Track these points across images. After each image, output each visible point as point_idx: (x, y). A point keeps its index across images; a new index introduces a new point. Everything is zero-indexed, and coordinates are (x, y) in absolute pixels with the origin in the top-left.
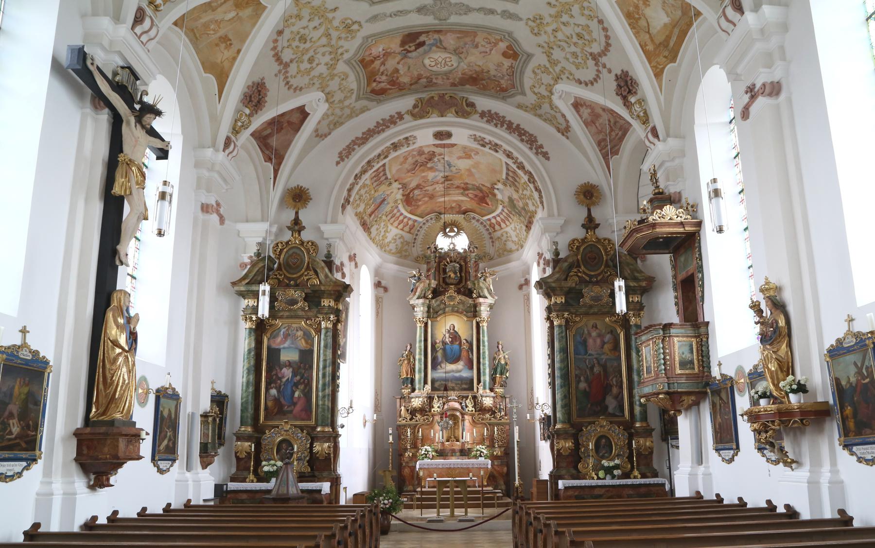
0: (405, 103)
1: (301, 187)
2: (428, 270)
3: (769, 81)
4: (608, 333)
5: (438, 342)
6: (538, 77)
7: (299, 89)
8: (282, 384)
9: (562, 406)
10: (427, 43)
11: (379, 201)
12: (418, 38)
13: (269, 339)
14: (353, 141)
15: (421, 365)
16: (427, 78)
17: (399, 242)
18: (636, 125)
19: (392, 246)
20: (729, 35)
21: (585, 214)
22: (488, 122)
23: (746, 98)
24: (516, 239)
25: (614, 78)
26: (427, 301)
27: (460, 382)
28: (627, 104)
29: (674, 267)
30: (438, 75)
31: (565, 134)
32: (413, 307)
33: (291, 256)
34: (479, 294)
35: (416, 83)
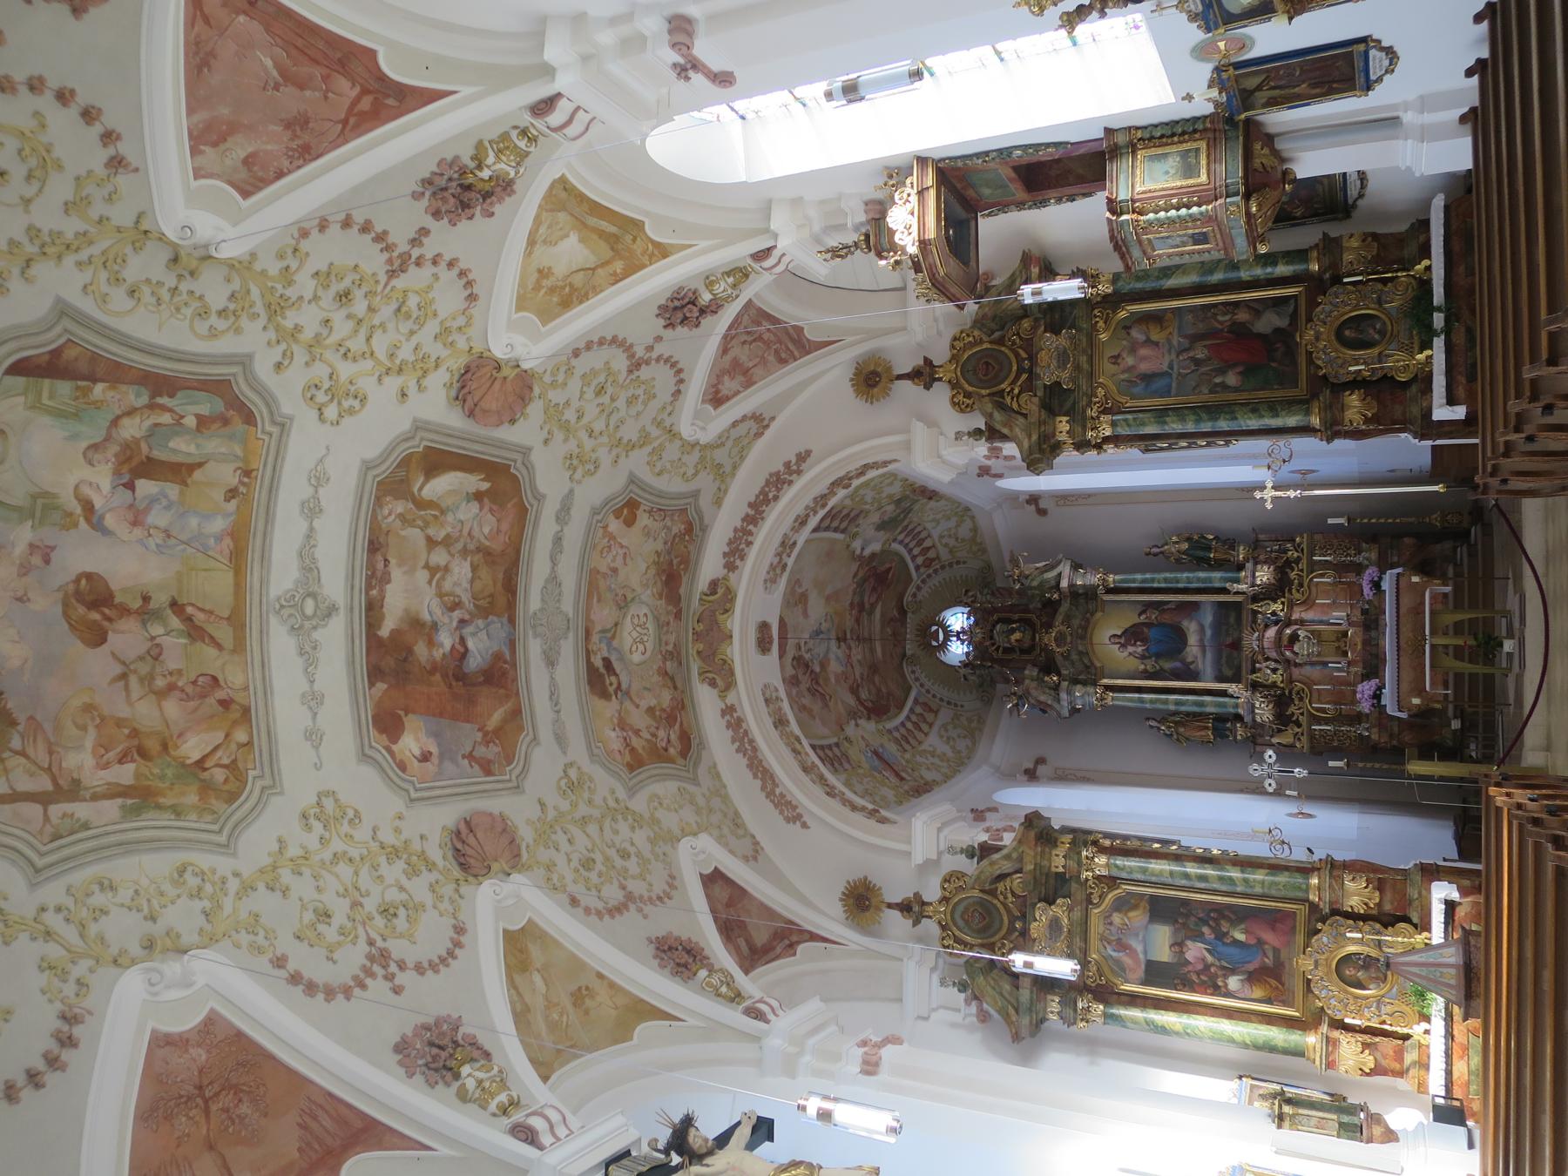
0: (706, 701)
1: (844, 894)
2: (1007, 681)
3: (667, 37)
5: (1142, 667)
6: (668, 466)
7: (673, 880)
8: (1217, 963)
9: (1273, 417)
10: (606, 655)
11: (877, 762)
12: (598, 670)
13: (1127, 981)
14: (767, 797)
16: (665, 659)
18: (748, 292)
19: (962, 745)
20: (594, 118)
21: (907, 384)
22: (742, 558)
23: (697, 78)
24: (954, 519)
25: (669, 332)
26: (1065, 684)
28: (713, 308)
29: (1003, 206)
30: (660, 640)
31: (765, 423)
32: (1074, 711)
33: (967, 922)
34: (1052, 588)
35: (672, 679)
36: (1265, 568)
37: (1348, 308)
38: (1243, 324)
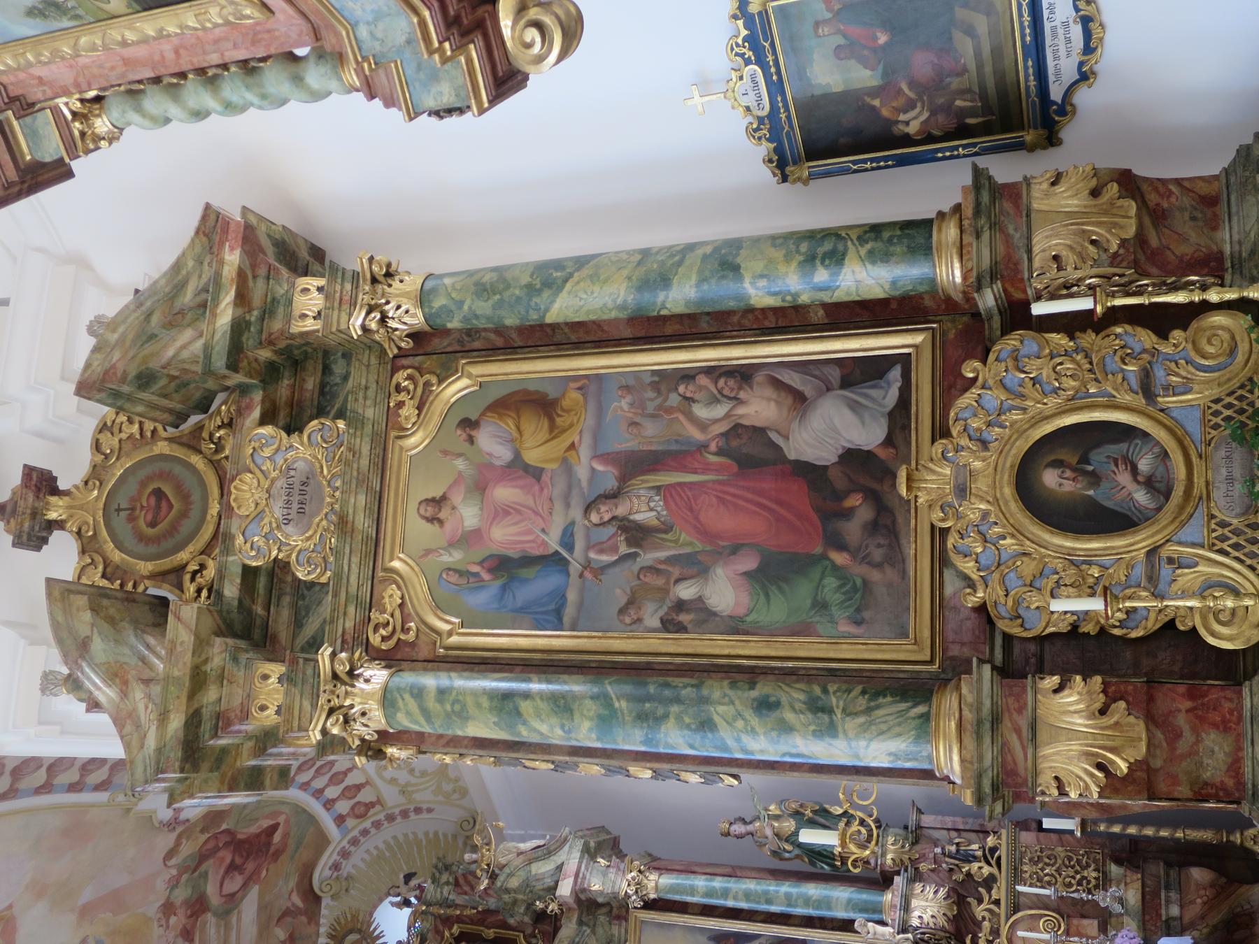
4: (471, 440)
9: (819, 734)
36: (930, 890)
37: (1053, 402)
38: (759, 432)
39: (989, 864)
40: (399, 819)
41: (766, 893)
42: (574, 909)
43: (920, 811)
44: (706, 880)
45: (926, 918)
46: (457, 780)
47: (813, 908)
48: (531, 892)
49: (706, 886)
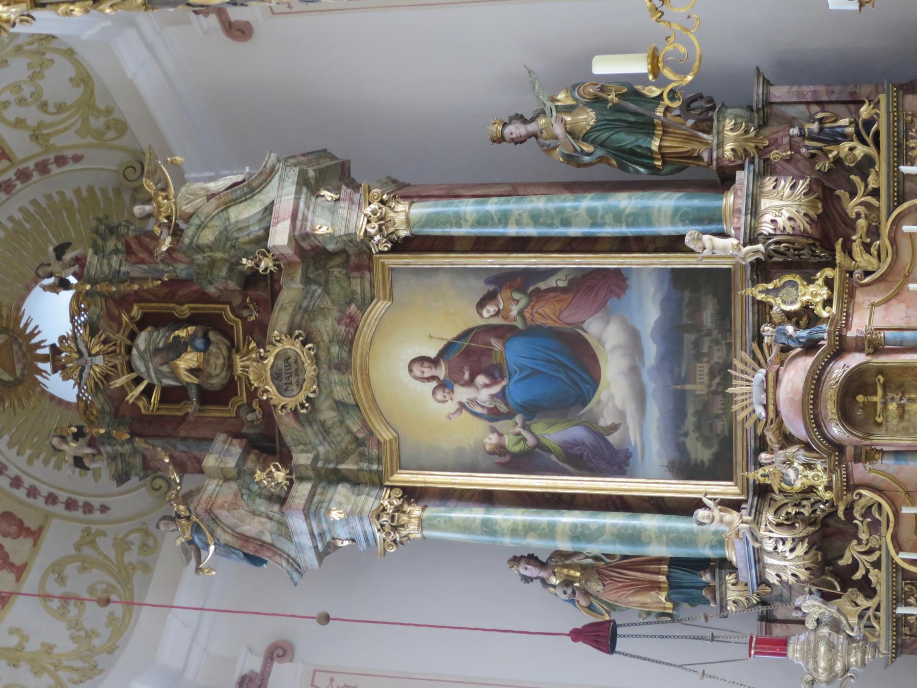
5: (492, 440)
15: (601, 530)
17: (77, 583)
27: (689, 338)
36: (785, 184)
39: (863, 142)
40: (36, 176)
41: (560, 211)
42: (295, 263)
43: (767, 83)
44: (476, 203)
45: (782, 221)
46: (109, 111)
47: (628, 225)
48: (233, 247)
49: (478, 212)
